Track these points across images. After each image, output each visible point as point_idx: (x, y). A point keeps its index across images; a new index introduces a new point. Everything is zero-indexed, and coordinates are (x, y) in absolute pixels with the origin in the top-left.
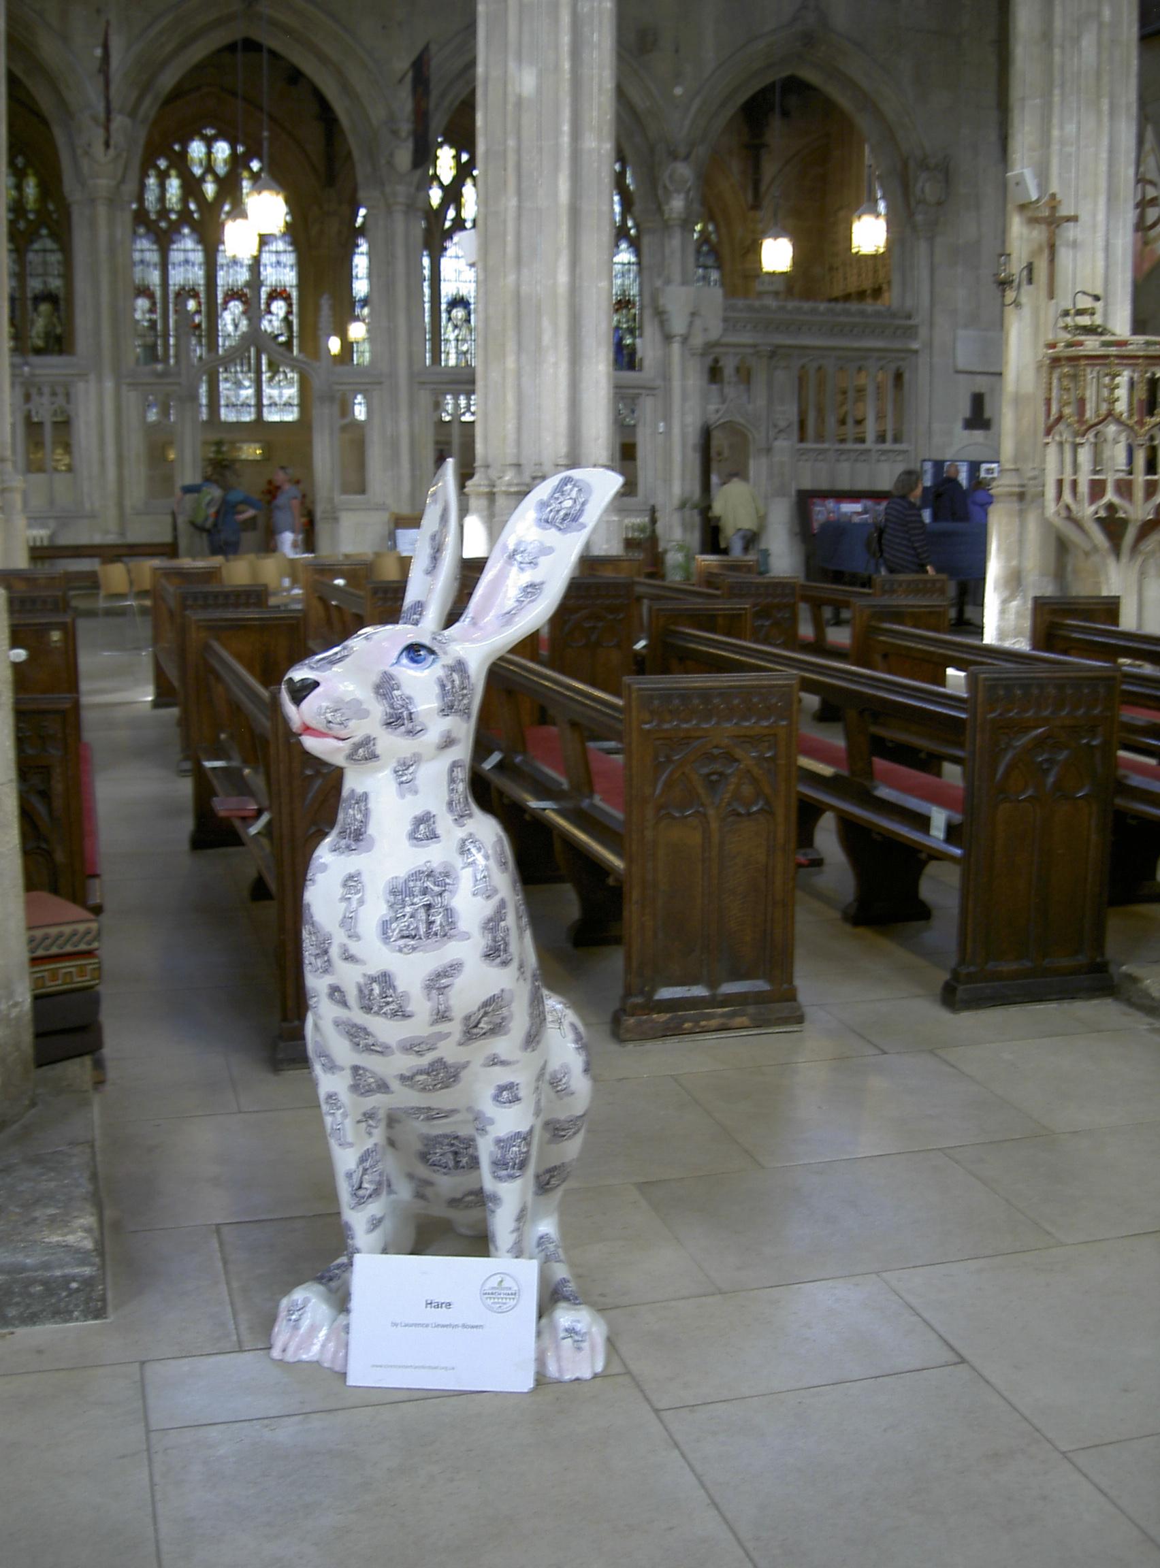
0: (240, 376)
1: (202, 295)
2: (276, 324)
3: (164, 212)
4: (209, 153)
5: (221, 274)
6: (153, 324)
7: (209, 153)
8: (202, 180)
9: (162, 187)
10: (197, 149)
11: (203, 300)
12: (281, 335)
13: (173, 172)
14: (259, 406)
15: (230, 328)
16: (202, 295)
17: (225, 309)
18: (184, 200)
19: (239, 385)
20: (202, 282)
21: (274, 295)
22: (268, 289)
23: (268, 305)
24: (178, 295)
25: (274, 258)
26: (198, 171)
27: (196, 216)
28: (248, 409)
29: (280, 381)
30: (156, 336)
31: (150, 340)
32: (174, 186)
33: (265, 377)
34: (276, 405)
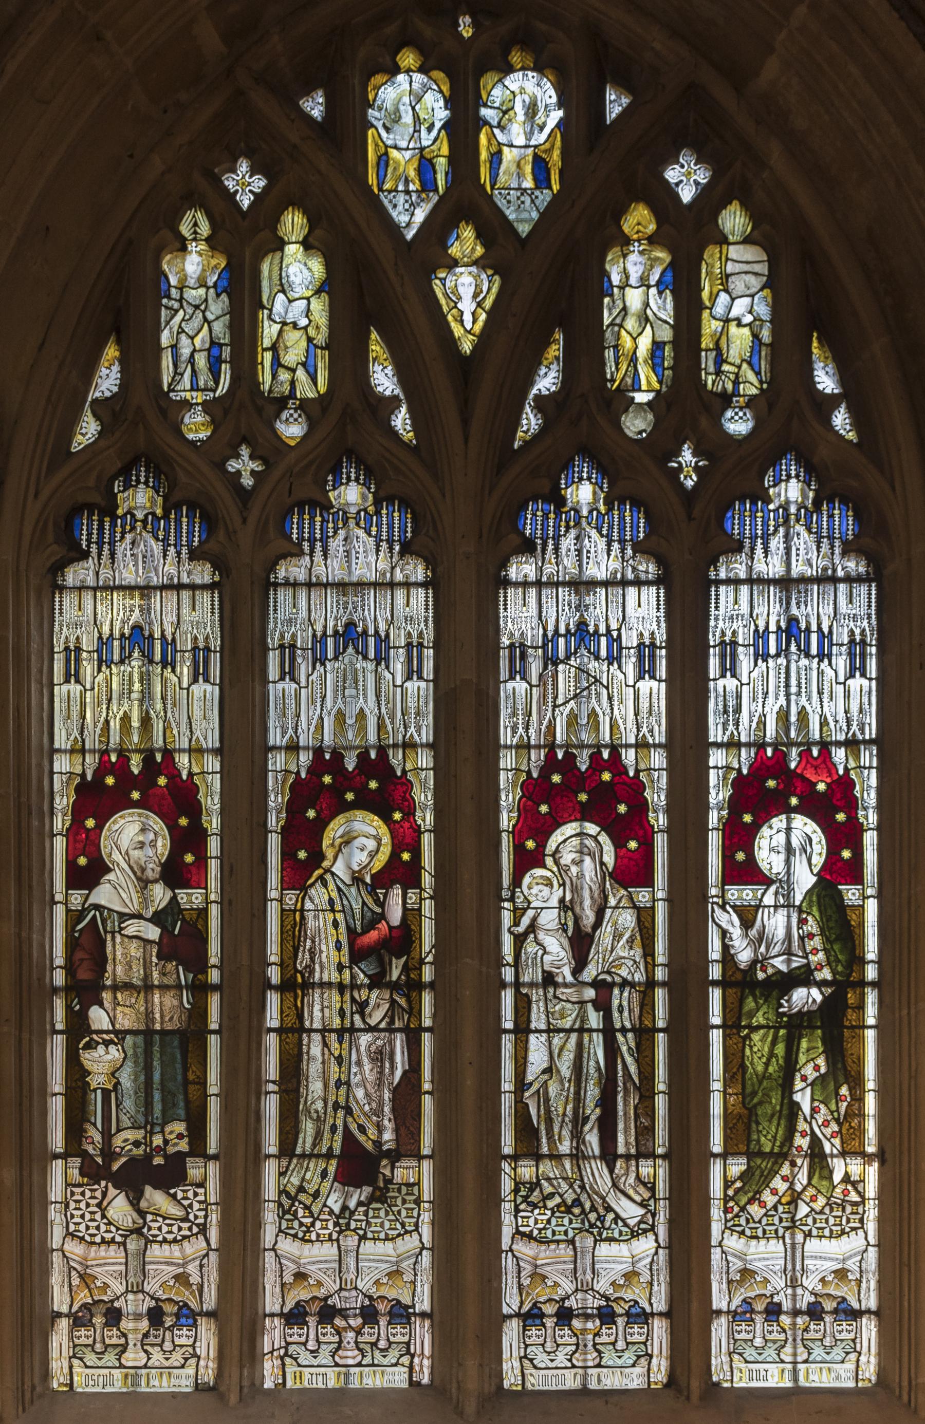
11: (426, 819)
12: (804, 977)
22: (745, 759)
28: (637, 1333)
29: (795, 1198)
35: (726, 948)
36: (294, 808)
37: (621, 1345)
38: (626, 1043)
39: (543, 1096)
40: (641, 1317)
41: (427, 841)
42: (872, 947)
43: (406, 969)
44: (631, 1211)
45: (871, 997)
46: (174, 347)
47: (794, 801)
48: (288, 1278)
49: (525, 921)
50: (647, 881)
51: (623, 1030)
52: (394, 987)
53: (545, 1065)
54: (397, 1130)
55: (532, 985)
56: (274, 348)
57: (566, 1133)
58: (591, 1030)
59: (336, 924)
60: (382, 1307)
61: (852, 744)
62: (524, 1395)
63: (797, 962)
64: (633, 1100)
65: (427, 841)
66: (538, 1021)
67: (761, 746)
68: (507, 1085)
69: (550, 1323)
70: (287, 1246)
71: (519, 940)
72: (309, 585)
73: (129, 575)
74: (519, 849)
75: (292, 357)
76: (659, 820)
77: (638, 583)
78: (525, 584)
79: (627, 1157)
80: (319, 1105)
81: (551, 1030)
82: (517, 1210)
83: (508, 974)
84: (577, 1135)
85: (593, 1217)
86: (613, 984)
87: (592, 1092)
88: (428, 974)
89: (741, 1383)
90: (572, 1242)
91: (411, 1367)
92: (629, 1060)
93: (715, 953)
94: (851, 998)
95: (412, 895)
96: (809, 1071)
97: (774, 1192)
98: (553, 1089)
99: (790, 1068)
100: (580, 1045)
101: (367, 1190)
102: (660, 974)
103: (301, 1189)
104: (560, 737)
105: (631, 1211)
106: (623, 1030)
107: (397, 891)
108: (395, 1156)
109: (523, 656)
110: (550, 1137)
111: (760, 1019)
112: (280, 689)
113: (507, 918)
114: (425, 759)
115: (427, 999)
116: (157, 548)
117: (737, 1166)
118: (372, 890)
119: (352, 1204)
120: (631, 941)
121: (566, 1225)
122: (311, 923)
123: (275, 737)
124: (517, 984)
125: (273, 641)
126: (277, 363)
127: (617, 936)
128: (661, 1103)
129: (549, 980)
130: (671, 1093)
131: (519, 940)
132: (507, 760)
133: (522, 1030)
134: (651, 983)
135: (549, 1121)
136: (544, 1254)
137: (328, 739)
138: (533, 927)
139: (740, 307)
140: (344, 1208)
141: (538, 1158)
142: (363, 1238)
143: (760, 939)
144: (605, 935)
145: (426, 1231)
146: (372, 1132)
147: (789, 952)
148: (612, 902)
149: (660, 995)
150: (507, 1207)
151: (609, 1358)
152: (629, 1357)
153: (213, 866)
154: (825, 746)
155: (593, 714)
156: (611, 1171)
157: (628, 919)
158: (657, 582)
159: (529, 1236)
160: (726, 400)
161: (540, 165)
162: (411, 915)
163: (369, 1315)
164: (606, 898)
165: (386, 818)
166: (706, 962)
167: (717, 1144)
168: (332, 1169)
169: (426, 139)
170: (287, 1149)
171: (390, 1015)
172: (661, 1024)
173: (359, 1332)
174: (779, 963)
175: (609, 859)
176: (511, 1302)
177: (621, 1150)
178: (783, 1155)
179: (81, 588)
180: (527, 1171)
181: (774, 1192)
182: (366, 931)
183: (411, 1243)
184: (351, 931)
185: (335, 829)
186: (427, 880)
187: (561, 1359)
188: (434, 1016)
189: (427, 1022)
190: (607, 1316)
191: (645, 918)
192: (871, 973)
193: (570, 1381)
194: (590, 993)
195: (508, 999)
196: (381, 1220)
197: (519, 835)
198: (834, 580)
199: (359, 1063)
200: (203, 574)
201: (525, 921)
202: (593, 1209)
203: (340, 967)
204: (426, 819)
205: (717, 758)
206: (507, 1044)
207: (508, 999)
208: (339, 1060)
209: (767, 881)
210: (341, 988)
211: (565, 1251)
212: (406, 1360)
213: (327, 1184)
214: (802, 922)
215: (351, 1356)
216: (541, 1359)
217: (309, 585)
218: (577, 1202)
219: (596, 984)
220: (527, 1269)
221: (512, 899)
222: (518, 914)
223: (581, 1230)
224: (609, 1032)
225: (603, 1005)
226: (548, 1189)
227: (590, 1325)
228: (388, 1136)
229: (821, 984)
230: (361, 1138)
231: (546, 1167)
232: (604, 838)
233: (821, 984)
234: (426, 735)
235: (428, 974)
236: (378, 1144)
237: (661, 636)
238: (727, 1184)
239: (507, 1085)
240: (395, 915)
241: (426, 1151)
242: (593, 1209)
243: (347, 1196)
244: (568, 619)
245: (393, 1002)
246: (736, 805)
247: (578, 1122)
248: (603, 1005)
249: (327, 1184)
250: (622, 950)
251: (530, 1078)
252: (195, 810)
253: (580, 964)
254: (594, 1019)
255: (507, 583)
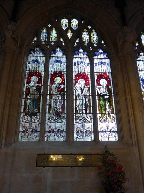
0: (85, 116)
1: (65, 76)
2: (102, 89)
3: (49, 42)
4: (69, 22)
5: (74, 67)
6: (39, 89)
7: (69, 22)
8: (67, 31)
9: (49, 33)
10: (64, 22)
11: (65, 78)
12: (106, 95)
13: (54, 29)
14: (96, 132)
15: (80, 92)
16: (65, 76)
17: (76, 83)
18: (58, 38)
19: (84, 121)
20: (65, 70)
21: (101, 76)
22: (98, 74)
23: (98, 81)
24: (52, 75)
25: (99, 60)
26: (65, 28)
27: (63, 44)
28: (90, 134)
30: (40, 95)
31: (36, 97)
32: (54, 34)
33: (99, 116)
34: (105, 131)
35: (97, 92)
36: (52, 77)
37: (88, 136)
38: (87, 101)
39: (78, 107)
40: (90, 132)
41: (66, 80)
42: (113, 93)
43: (63, 93)
44: (89, 120)
45: (113, 97)
46: (42, 37)
47: (103, 78)
48: (49, 127)
49: (76, 88)
50: (89, 85)
51: (87, 100)
52: (62, 95)
53: (78, 103)
54: (62, 110)
55: (77, 95)
56: (52, 38)
57: (81, 111)
58: (83, 100)
59: (55, 88)
60: (60, 131)
61: (109, 73)
62: (77, 142)
63: (105, 93)
64: (88, 107)
65: (66, 80)
66: (78, 98)
67: (100, 73)
68: (74, 105)
69: (80, 133)
70: (49, 123)
71: (75, 90)
72: (54, 57)
73: (36, 55)
74: (75, 81)
75: (53, 38)
76: (90, 79)
77: (87, 58)
78: (76, 58)
79: (88, 114)
80: (53, 107)
81: (79, 100)
82: (76, 119)
83: (74, 94)
84: (82, 111)
85: (84, 120)
86: (86, 95)
87: (84, 107)
88: (65, 94)
89: (103, 140)
90: (82, 123)
91: (63, 138)
92: (88, 103)
93: (96, 92)
94: (111, 97)
95: (64, 85)
96: (107, 105)
97: (105, 118)
98: (79, 106)
99: (105, 104)
100: (82, 101)
101: (58, 117)
102: (91, 94)
103: (51, 117)
104: (79, 71)
105: (89, 120)
106: (87, 100)
107: (62, 85)
108: (62, 113)
109: (75, 64)
110: (79, 111)
111: (101, 99)
112: (50, 66)
113: (74, 88)
114: (65, 73)
115: (65, 96)
116: (39, 53)
117: (100, 115)
118: (60, 85)
119: (56, 119)
120: (87, 91)
121: (81, 121)
122: (53, 88)
123: (50, 70)
124: (75, 95)
125: (50, 61)
126: (52, 39)
127: (86, 90)
128: (91, 108)
129: (79, 94)
130: (92, 107)
131: (75, 90)
132: (74, 73)
133: (76, 100)
134: (90, 95)
135: (79, 109)
136: (79, 125)
137: (55, 70)
138: (77, 89)
139: (95, 37)
140: (56, 119)
141: (78, 114)
142: (58, 122)
143: (101, 91)
144: (85, 90)
145: (65, 122)
146: (59, 110)
147: (104, 92)
148: (85, 87)
149: (91, 96)
150: (75, 119)
151: (87, 137)
152: (89, 137)
153: (43, 82)
154: (106, 73)
155: (83, 69)
156: (86, 115)
157: (87, 89)
158: (89, 58)
159: (77, 123)
160: (94, 44)
161: (76, 26)
162: (64, 88)
163: (58, 132)
164: (84, 86)
165: (61, 78)
166: (96, 93)
167: (98, 112)
168: (54, 115)
169: (66, 23)
170: (49, 112)
171: (61, 98)
172: (91, 99)
173: (57, 134)
174: (103, 93)
175: (85, 83)
176: (75, 130)
177: (87, 113)
178: (105, 114)
179: (31, 56)
180: (77, 115)
181: (105, 118)
182: (59, 89)
183: (63, 123)
184: (57, 89)
185: (56, 79)
186: (65, 84)
187: (81, 137)
188: (66, 98)
189: (65, 99)
190: (86, 132)
191: (89, 88)
192: (113, 95)
193: (82, 140)
194: (83, 96)
195: (74, 96)
196: (60, 121)
197: (75, 80)
198: (106, 59)
199: (58, 103)
200: (43, 55)
201: (76, 88)
202: (84, 119)
203: (56, 93)
204: (65, 78)
205: (95, 73)
206: (74, 101)
207: (74, 96)
208: (55, 102)
209: (101, 85)
210: (56, 95)
211: (81, 124)
212: (62, 137)
213: (54, 116)
214: (105, 89)
215: (56, 137)
216: (79, 137)
217: (54, 57)
218: (83, 119)
219: (84, 95)
220: (77, 126)
221: (75, 86)
222: (75, 88)
223: (83, 122)
224: (85, 100)
225: (85, 97)
226: (79, 117)
227: (84, 133)
228: (61, 111)
229: (108, 96)
230: (58, 111)
231: (79, 115)
232: (84, 81)
233: (108, 96)
234: (66, 70)
235: (65, 94)
236: (60, 112)
237: (89, 63)
238: (99, 117)
239: (74, 105)
240: (62, 87)
241: (65, 113)
242: (84, 119)
243: (56, 118)
244: (80, 61)
245: (62, 96)
246: (97, 78)
247: (82, 110)
248: (85, 97)
249: (54, 116)
250: (87, 92)
251: (77, 104)
252: (41, 76)
253: (82, 93)
254: (84, 99)
255: (74, 57)
